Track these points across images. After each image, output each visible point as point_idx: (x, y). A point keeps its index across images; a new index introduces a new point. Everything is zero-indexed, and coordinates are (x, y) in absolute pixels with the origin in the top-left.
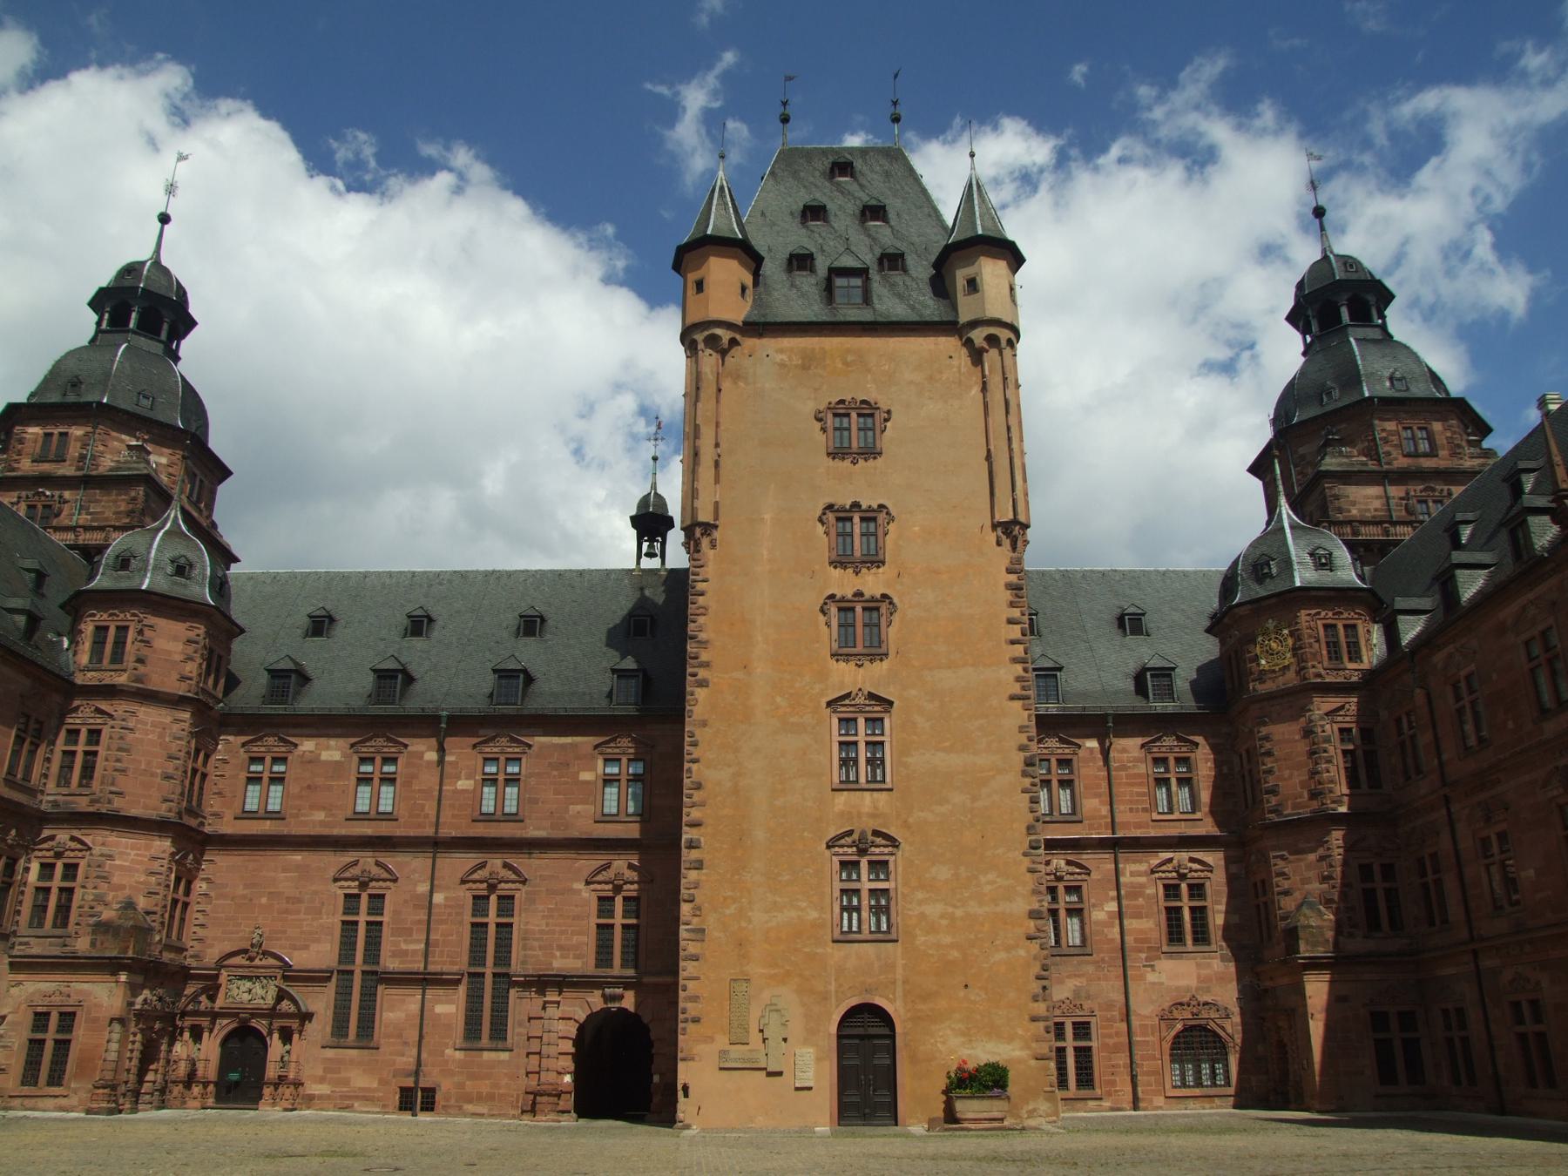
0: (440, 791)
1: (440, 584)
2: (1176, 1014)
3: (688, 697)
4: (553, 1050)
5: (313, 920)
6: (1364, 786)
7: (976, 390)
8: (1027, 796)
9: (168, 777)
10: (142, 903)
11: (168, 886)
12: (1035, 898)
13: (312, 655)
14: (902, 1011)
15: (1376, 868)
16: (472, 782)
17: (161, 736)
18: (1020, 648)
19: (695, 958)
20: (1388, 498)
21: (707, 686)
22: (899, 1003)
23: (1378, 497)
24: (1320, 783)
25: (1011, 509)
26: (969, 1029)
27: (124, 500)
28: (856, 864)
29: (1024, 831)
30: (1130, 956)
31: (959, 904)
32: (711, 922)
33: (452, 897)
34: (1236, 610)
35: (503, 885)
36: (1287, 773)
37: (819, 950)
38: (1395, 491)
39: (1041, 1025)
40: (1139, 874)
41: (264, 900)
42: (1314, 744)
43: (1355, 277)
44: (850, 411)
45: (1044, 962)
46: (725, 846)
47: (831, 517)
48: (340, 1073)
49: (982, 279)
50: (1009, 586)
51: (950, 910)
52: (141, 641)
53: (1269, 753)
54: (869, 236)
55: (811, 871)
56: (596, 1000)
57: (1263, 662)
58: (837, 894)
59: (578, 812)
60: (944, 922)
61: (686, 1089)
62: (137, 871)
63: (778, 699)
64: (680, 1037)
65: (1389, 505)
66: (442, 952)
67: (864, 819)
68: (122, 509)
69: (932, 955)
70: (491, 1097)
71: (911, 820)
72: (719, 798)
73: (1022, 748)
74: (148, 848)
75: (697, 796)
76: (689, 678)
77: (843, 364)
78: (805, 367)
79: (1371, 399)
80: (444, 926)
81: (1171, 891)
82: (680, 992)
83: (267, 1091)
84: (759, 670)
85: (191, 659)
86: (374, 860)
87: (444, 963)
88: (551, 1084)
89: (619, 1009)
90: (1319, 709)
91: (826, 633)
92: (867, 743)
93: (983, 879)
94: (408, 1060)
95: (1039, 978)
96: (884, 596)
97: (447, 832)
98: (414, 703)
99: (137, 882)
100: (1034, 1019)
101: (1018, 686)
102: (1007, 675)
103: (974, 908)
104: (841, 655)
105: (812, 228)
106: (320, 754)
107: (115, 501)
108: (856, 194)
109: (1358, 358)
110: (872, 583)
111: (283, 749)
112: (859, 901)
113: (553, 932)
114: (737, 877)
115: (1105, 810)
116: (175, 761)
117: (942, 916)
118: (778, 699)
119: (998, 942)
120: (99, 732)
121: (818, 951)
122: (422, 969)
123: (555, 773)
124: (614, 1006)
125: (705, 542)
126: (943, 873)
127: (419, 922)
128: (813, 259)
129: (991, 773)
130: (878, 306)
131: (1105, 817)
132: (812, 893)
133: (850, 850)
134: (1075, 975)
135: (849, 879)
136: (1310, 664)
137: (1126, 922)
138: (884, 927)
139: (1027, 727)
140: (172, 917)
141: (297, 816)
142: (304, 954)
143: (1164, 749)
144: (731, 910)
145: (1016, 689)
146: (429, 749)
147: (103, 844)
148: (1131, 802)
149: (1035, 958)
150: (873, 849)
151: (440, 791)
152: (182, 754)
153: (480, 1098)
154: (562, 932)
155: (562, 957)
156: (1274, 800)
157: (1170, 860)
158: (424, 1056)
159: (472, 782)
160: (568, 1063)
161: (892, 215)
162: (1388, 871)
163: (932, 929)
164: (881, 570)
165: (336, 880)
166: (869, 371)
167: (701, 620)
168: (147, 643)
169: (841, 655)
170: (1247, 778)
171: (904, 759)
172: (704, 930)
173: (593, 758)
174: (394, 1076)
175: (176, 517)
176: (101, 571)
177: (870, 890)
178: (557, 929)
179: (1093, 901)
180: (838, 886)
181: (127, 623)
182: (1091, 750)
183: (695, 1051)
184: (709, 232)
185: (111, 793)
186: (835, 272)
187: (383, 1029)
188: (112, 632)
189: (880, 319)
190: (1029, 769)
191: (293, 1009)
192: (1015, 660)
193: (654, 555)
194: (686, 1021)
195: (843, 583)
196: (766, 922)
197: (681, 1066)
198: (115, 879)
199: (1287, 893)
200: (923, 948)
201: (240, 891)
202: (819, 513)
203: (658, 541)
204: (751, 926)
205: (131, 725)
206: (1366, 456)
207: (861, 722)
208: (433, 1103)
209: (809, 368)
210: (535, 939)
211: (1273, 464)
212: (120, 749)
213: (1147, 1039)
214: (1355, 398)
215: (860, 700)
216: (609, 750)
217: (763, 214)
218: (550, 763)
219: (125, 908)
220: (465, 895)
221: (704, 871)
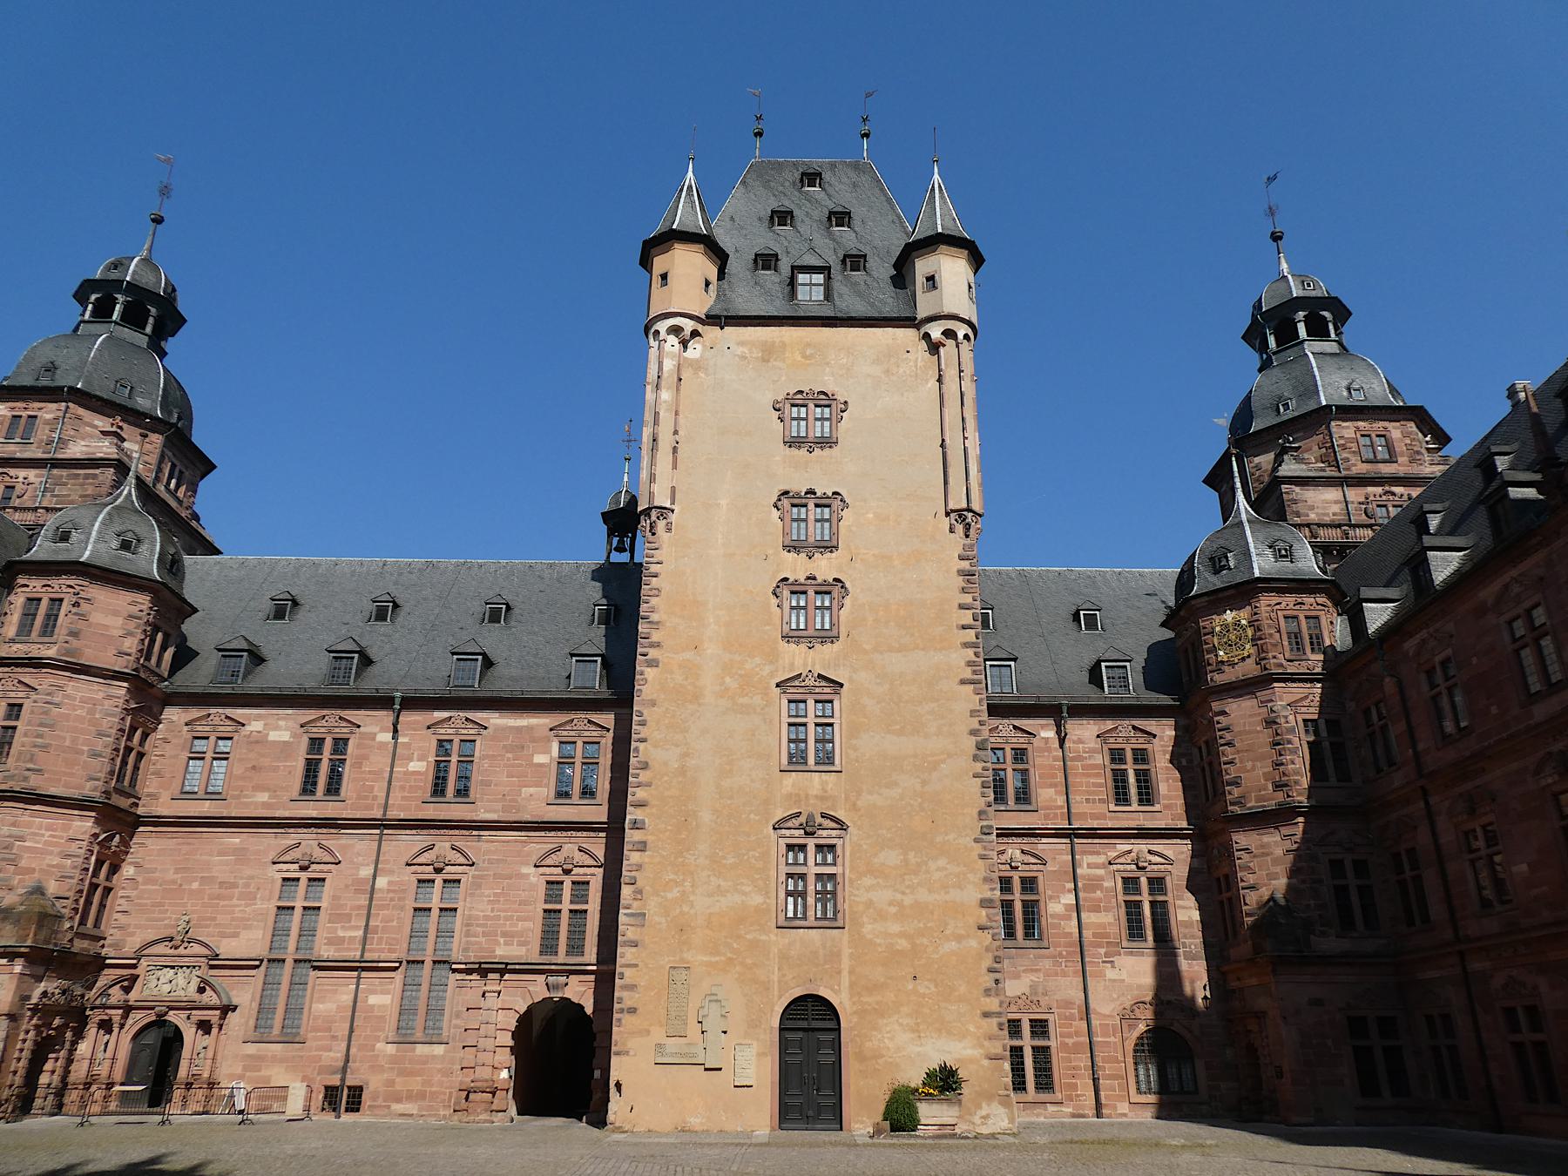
0: (391, 772)
1: (410, 573)
2: (1138, 1013)
3: (637, 677)
4: (489, 1044)
5: (247, 905)
6: (1333, 781)
7: (933, 384)
8: (979, 781)
9: (95, 755)
10: (52, 888)
11: (87, 869)
12: (987, 887)
13: (269, 637)
14: (847, 1004)
16: (425, 763)
17: (91, 712)
18: (972, 632)
20: (1346, 502)
23: (1336, 502)
25: (964, 497)
26: (917, 1024)
27: (91, 484)
28: (803, 848)
29: (976, 816)
30: (1088, 951)
31: (907, 891)
32: (652, 906)
33: (395, 879)
34: (1193, 602)
35: (448, 868)
36: (1249, 765)
37: (764, 937)
38: (1355, 494)
39: (994, 1021)
40: (1097, 866)
41: (195, 885)
42: (1277, 734)
43: (1313, 294)
44: (806, 402)
45: (997, 953)
46: (669, 828)
47: (786, 502)
48: (259, 1071)
49: (940, 277)
50: (961, 573)
51: (899, 896)
52: (76, 614)
53: (1229, 744)
54: (834, 240)
56: (537, 989)
57: (1221, 653)
58: (783, 878)
59: (531, 795)
60: (893, 910)
61: (618, 1086)
62: (51, 853)
63: (728, 680)
64: (615, 1029)
65: (1348, 509)
66: (381, 939)
67: (812, 802)
68: (88, 492)
69: (880, 945)
70: (421, 1096)
71: (859, 803)
72: (666, 778)
73: (973, 733)
74: (66, 828)
75: (644, 776)
76: (639, 657)
77: (803, 357)
78: (765, 360)
79: (1328, 407)
80: (386, 912)
81: (1130, 884)
82: (617, 980)
83: (177, 1094)
84: (709, 651)
85: (130, 634)
86: (317, 842)
87: (382, 951)
88: (487, 1081)
89: (561, 998)
90: (1281, 700)
91: (776, 615)
92: (817, 725)
93: (932, 865)
94: (336, 1055)
95: (990, 970)
96: (835, 580)
97: (392, 814)
98: (371, 683)
99: (49, 866)
100: (986, 1015)
101: (969, 670)
102: (959, 659)
103: (923, 895)
104: (792, 637)
105: (779, 232)
106: (268, 734)
107: (82, 485)
108: (823, 203)
109: (1315, 369)
110: (824, 566)
111: (229, 729)
112: (805, 886)
113: (498, 918)
114: (680, 860)
115: (1061, 801)
116: (104, 738)
117: (891, 904)
118: (728, 680)
119: (947, 932)
120: (21, 705)
122: (358, 958)
123: (510, 755)
124: (557, 995)
125: (661, 524)
126: (891, 857)
127: (359, 908)
128: (777, 260)
129: (942, 757)
130: (838, 303)
131: (1061, 807)
132: (757, 877)
133: (797, 833)
134: (1032, 970)
135: (796, 864)
136: (1270, 655)
137: (1083, 915)
138: (830, 914)
140: (88, 903)
141: (238, 797)
142: (234, 942)
143: (1120, 740)
144: (674, 894)
145: (968, 673)
146: (383, 730)
147: (14, 824)
148: (1088, 792)
149: (987, 949)
150: (820, 832)
151: (391, 772)
152: (114, 731)
153: (410, 1097)
154: (506, 919)
155: (506, 944)
156: (1236, 792)
157: (1130, 852)
158: (353, 1051)
159: (425, 763)
160: (506, 1058)
161: (856, 222)
162: (1361, 867)
163: (882, 916)
165: (274, 863)
166: (828, 364)
167: (654, 601)
168: (83, 617)
169: (792, 637)
170: (1207, 769)
172: (644, 914)
173: (549, 741)
174: (318, 1074)
175: (130, 493)
176: (38, 542)
178: (502, 914)
179: (1049, 892)
180: (784, 869)
181: (62, 596)
182: (1047, 739)
183: (629, 1046)
184: (674, 227)
185: (29, 770)
186: (797, 269)
187: (311, 1021)
188: (44, 604)
189: (839, 315)
190: (980, 753)
191: (215, 1001)
192: (966, 645)
193: (625, 550)
194: (622, 1011)
195: (797, 567)
196: (708, 908)
197: (614, 1060)
198: (23, 862)
199: (1252, 888)
200: (869, 936)
201: (171, 875)
203: (628, 537)
204: (692, 911)
205: (56, 700)
206: (1323, 462)
207: (811, 703)
208: (360, 1103)
209: (768, 361)
210: (478, 925)
211: (1231, 461)
212: (41, 725)
213: (1108, 1040)
214: (1312, 406)
216: (565, 733)
217: (732, 219)
218: (505, 746)
219: (31, 893)
220: (409, 877)
221: (646, 853)
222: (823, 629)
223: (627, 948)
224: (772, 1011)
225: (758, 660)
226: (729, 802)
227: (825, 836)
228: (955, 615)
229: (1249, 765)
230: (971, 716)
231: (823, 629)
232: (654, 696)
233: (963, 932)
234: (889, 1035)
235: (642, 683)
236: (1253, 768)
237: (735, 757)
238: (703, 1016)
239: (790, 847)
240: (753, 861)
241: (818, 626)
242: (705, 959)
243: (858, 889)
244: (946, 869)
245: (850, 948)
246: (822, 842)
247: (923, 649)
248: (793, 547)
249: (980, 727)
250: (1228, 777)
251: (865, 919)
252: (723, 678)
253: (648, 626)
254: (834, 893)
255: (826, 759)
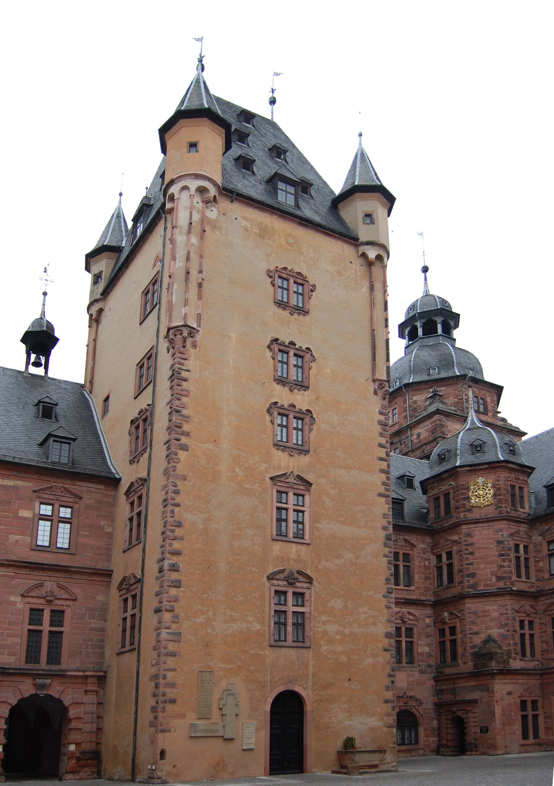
15: (526, 623)
19: (173, 654)
21: (187, 450)
22: (309, 690)
24: (505, 572)
28: (285, 593)
31: (347, 626)
36: (482, 566)
37: (261, 652)
39: (390, 705)
46: (197, 572)
55: (257, 596)
58: (273, 613)
60: (338, 637)
67: (291, 563)
71: (320, 567)
72: (194, 536)
75: (178, 532)
92: (294, 510)
93: (361, 610)
95: (390, 676)
100: (386, 702)
103: (356, 629)
112: (285, 619)
117: (337, 633)
118: (237, 469)
119: (368, 652)
121: (259, 653)
132: (257, 611)
133: (282, 583)
135: (279, 604)
139: (388, 515)
144: (201, 620)
149: (388, 663)
164: (306, 393)
167: (184, 399)
169: (280, 446)
171: (317, 525)
172: (180, 634)
177: (293, 612)
180: (274, 608)
200: (325, 653)
202: (268, 342)
215: (291, 480)
221: (181, 589)
222: (297, 444)
223: (168, 657)
224: (266, 701)
225: (257, 459)
226: (238, 558)
227: (301, 586)
228: (376, 450)
229: (482, 566)
230: (384, 518)
231: (297, 444)
232: (186, 473)
233: (375, 652)
234: (334, 715)
235: (176, 461)
236: (485, 568)
237: (242, 526)
238: (223, 705)
239: (276, 592)
240: (254, 600)
241: (295, 442)
242: (223, 666)
243: (318, 623)
244: (368, 613)
245: (313, 661)
246: (298, 590)
247: (358, 469)
248: (281, 381)
249: (388, 526)
250: (468, 572)
251: (322, 643)
252: (234, 468)
253: (181, 418)
254: (303, 625)
255: (299, 535)
